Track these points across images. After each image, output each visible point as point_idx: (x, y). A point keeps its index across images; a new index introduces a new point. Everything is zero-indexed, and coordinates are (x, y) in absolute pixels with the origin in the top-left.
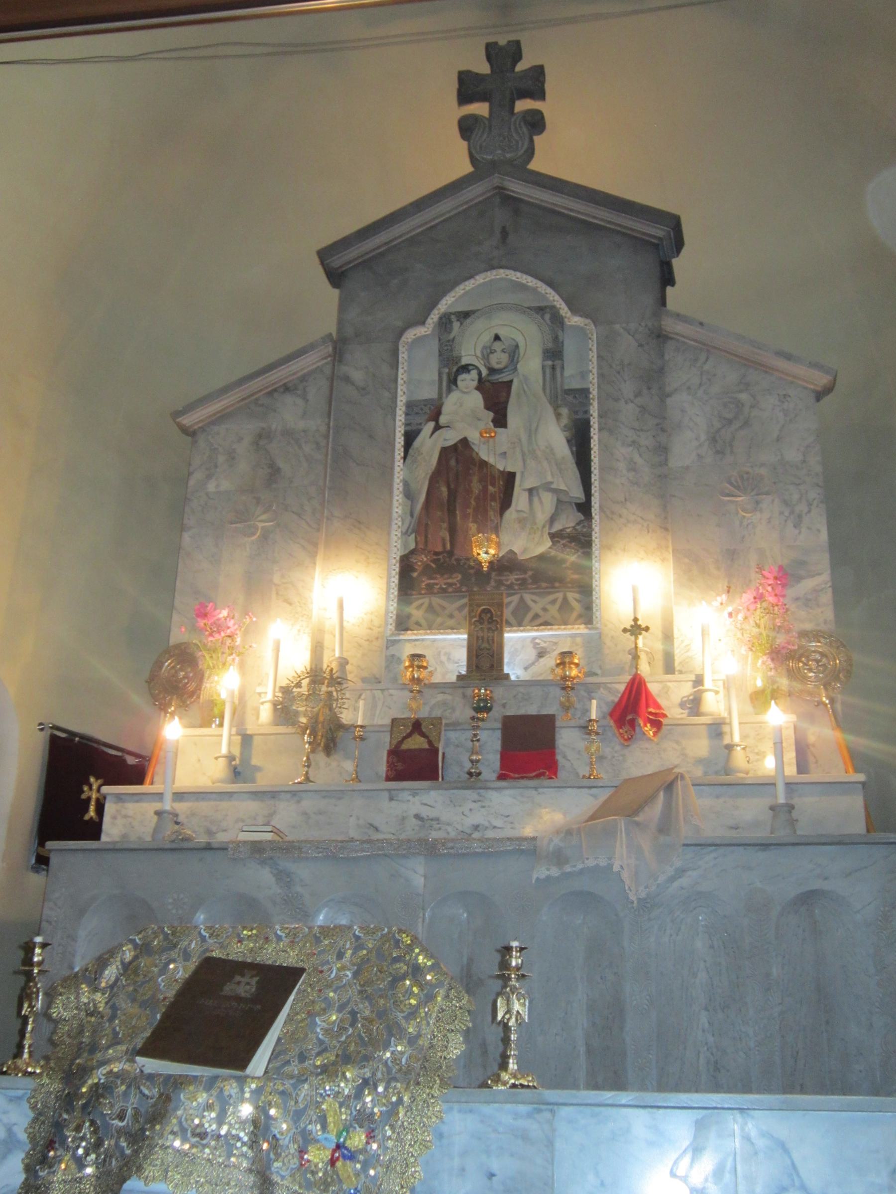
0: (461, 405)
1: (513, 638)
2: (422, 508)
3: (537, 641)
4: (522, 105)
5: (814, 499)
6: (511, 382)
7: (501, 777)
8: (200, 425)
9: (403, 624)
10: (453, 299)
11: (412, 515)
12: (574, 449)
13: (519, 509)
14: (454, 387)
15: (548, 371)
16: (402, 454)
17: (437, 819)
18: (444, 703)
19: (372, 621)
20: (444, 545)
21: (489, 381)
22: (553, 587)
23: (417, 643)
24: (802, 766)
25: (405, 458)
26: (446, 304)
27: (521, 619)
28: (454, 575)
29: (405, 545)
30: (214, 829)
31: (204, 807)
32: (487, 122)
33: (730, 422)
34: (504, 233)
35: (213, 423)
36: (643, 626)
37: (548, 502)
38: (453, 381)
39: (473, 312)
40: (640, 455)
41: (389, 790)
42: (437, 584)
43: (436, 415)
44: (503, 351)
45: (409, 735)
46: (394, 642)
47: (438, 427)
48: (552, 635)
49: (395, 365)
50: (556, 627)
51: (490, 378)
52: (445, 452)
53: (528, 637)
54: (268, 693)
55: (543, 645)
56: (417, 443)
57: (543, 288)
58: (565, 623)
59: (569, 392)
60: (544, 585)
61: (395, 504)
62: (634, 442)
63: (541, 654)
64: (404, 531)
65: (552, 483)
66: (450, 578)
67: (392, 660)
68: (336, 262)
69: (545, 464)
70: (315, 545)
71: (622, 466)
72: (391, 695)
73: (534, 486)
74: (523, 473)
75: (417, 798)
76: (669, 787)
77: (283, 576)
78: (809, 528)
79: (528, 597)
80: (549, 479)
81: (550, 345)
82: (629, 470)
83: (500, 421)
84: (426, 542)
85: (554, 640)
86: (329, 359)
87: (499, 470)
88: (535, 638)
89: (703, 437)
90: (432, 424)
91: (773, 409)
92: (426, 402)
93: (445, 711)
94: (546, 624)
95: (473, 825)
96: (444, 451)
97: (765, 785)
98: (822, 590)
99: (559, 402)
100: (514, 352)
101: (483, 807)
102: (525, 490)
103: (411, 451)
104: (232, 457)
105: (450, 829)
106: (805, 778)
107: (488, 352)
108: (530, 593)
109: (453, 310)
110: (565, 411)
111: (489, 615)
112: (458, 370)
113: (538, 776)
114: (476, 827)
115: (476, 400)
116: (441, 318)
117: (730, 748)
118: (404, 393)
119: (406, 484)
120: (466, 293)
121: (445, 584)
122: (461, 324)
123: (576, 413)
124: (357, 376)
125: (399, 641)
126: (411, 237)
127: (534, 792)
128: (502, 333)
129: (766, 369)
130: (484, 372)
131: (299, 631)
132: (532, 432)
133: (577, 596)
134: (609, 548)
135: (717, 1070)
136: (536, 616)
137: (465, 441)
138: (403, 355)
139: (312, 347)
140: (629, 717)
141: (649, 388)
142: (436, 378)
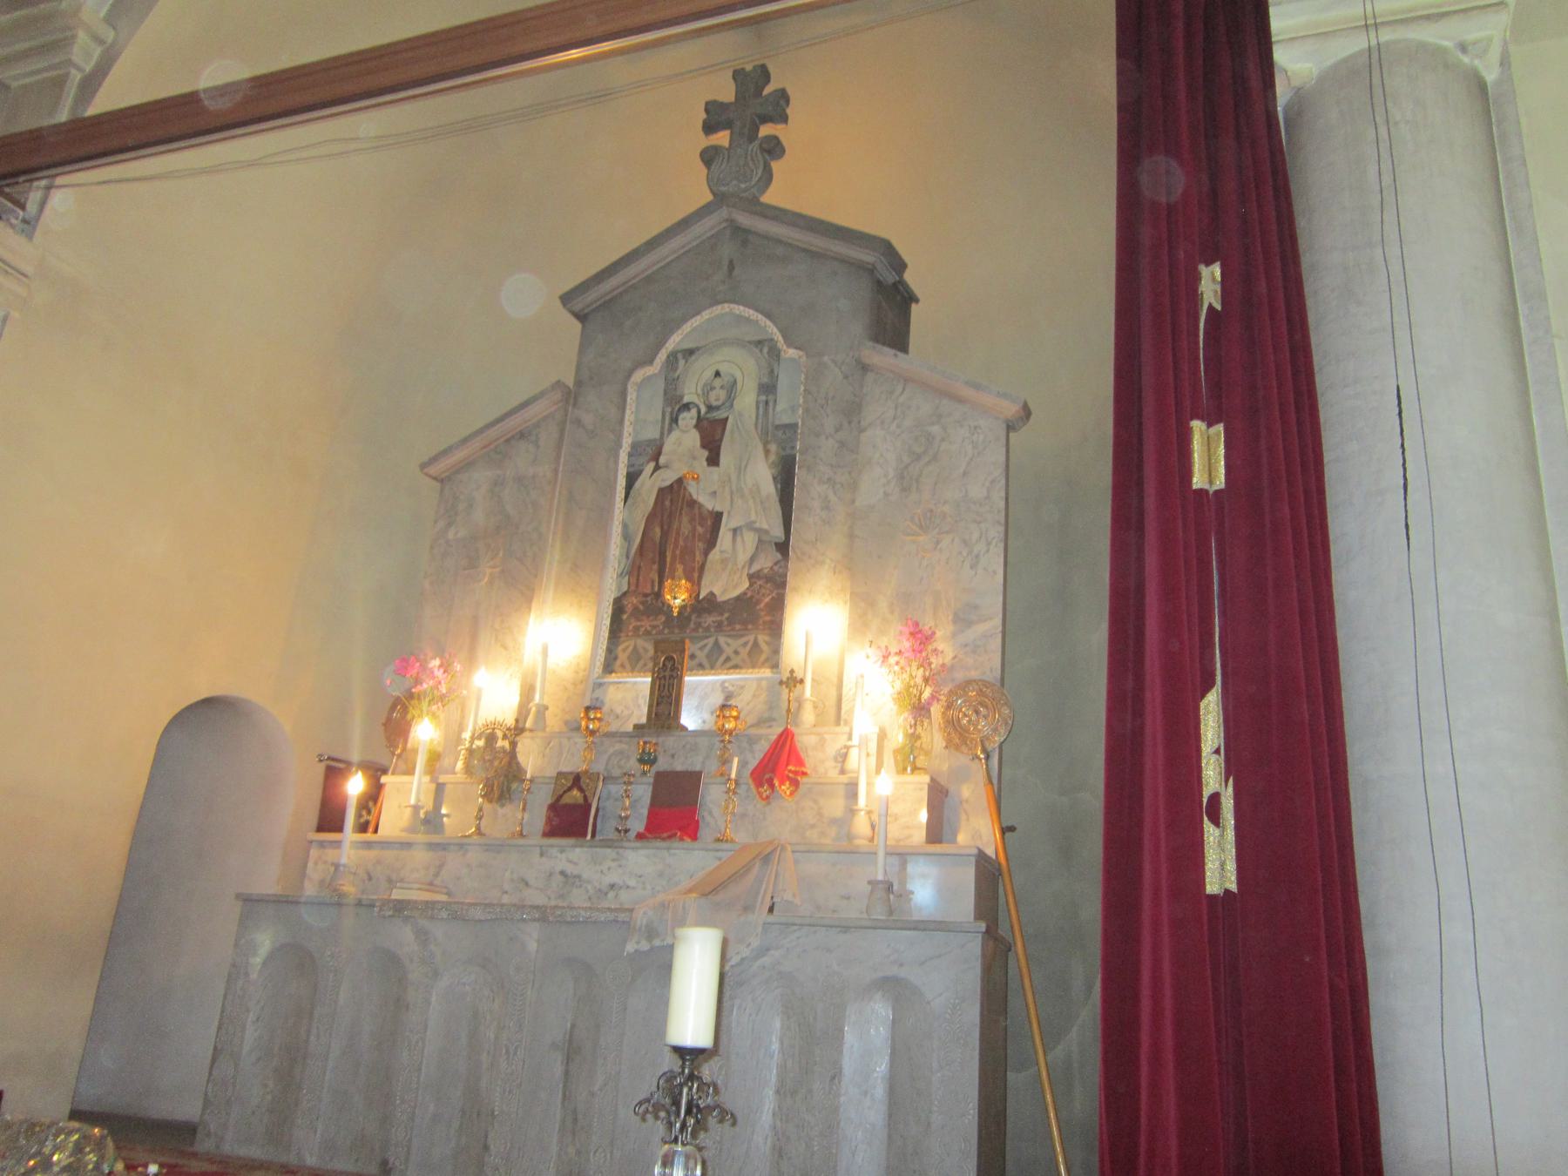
0: (680, 444)
2: (637, 549)
3: (726, 685)
4: (765, 130)
5: (994, 538)
6: (727, 419)
8: (447, 474)
10: (680, 337)
11: (627, 557)
12: (779, 486)
13: (723, 549)
14: (674, 425)
15: (761, 405)
16: (623, 496)
17: (579, 877)
18: (621, 752)
19: (578, 664)
20: (653, 586)
21: (707, 419)
22: (746, 629)
23: (620, 686)
26: (674, 342)
27: (713, 661)
28: (659, 617)
29: (619, 587)
30: (394, 877)
32: (726, 152)
33: (918, 457)
34: (731, 266)
35: (458, 472)
36: (798, 678)
37: (750, 539)
38: (675, 420)
39: (698, 349)
40: (835, 493)
41: (541, 847)
42: (642, 626)
43: (656, 457)
44: (722, 387)
45: (570, 789)
46: (601, 685)
47: (657, 468)
48: (741, 679)
49: (622, 408)
50: (744, 671)
51: (709, 416)
52: (662, 492)
53: (717, 681)
55: (731, 688)
56: (637, 484)
58: (754, 667)
59: (777, 427)
60: (738, 627)
61: (613, 546)
62: (829, 479)
64: (619, 573)
65: (754, 522)
66: (656, 619)
68: (578, 305)
69: (751, 502)
72: (576, 743)
73: (739, 525)
74: (729, 513)
75: (564, 855)
77: (502, 621)
78: (985, 569)
79: (722, 640)
80: (753, 518)
81: (765, 380)
82: (822, 509)
83: (713, 460)
84: (637, 586)
85: (742, 683)
86: (560, 405)
87: (708, 511)
88: (724, 682)
89: (891, 474)
90: (652, 465)
91: (963, 442)
92: (650, 442)
93: (621, 760)
94: (736, 667)
95: (610, 885)
96: (661, 491)
98: (991, 636)
99: (769, 438)
100: (731, 388)
101: (620, 866)
102: (729, 530)
103: (632, 492)
105: (589, 887)
108: (725, 636)
109: (680, 348)
110: (773, 447)
111: (671, 663)
112: (679, 410)
113: (670, 837)
114: (612, 886)
116: (668, 357)
118: (630, 434)
119: (625, 526)
120: (694, 330)
121: (650, 626)
122: (686, 362)
123: (784, 449)
124: (588, 419)
125: (605, 683)
126: (647, 276)
127: (665, 853)
128: (723, 368)
129: (960, 400)
130: (703, 410)
131: (511, 675)
132: (741, 470)
133: (767, 638)
135: (781, 1156)
136: (728, 659)
138: (631, 396)
139: (542, 394)
140: (767, 776)
141: (850, 423)
142: (660, 417)
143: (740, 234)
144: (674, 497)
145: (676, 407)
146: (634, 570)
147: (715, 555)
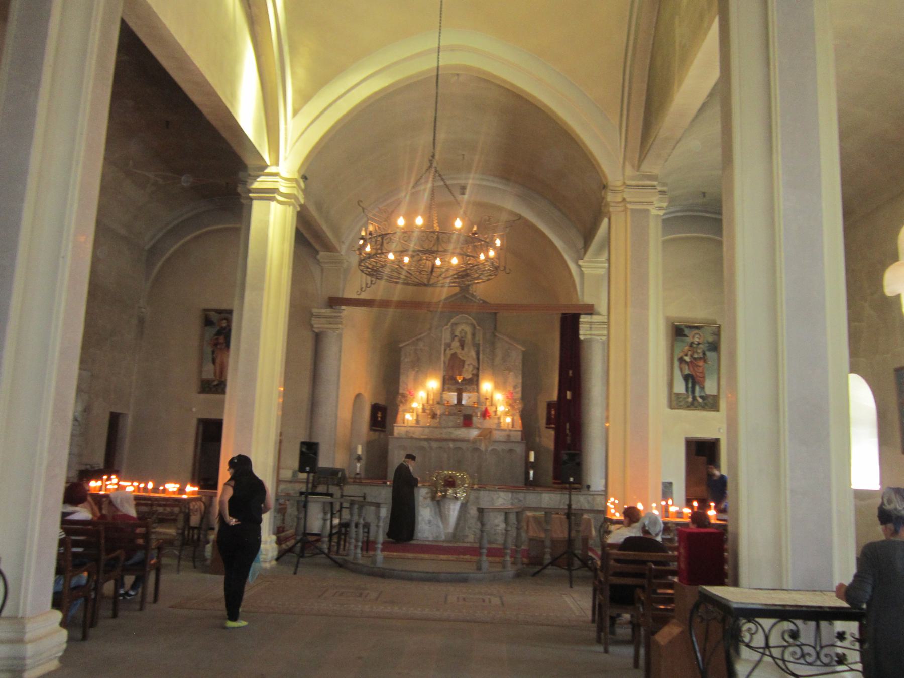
1: (464, 395)
7: (464, 426)
9: (443, 389)
24: (513, 426)
26: (453, 321)
31: (413, 429)
37: (471, 368)
47: (451, 349)
54: (420, 407)
76: (490, 432)
83: (463, 349)
94: (470, 392)
97: (505, 430)
100: (466, 333)
106: (513, 429)
107: (460, 333)
144: (454, 355)
145: (454, 337)
147: (464, 370)
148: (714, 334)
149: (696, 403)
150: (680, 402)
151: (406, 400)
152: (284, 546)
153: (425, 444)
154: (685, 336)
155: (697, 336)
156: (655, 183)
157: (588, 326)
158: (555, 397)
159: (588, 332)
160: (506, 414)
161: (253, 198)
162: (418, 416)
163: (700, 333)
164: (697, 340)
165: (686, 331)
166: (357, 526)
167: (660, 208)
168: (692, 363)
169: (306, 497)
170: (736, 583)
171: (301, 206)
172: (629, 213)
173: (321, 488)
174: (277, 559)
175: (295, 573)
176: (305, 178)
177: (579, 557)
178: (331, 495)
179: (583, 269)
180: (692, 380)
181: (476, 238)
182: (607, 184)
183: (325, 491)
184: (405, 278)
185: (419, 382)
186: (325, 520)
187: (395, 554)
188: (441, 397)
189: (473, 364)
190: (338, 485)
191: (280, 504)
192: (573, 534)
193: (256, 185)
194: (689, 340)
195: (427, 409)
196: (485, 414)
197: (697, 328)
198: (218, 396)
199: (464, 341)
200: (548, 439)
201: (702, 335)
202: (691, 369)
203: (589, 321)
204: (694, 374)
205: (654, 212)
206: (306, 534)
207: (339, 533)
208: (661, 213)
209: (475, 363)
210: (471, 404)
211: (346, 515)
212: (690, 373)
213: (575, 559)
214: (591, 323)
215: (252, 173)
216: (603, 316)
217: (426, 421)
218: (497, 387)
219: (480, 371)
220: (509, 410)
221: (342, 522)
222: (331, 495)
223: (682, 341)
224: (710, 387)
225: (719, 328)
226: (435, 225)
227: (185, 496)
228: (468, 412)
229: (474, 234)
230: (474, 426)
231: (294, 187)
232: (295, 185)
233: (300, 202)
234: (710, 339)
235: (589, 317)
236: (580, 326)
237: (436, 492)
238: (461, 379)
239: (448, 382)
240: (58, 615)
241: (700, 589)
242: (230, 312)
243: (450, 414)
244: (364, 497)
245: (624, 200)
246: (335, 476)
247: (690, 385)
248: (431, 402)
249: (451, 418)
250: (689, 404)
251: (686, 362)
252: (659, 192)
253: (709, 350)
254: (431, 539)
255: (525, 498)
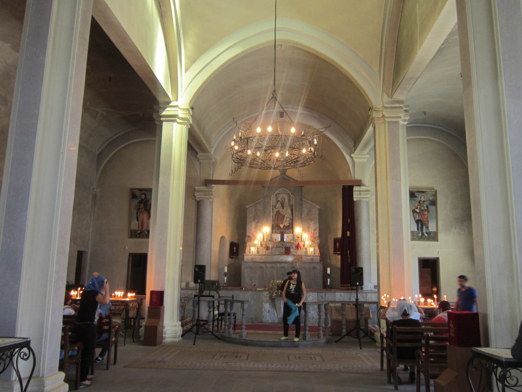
9: (272, 233)
24: (314, 253)
25: (272, 212)
31: (255, 256)
37: (288, 220)
38: (278, 203)
47: (276, 209)
52: (277, 212)
57: (289, 192)
63: (288, 237)
67: (271, 238)
70: (263, 225)
71: (297, 216)
76: (302, 257)
83: (283, 208)
90: (275, 208)
94: (288, 234)
97: (310, 256)
100: (285, 199)
104: (252, 212)
106: (315, 255)
107: (281, 199)
110: (290, 207)
115: (280, 205)
117: (307, 252)
119: (272, 215)
124: (266, 202)
128: (283, 197)
134: (295, 226)
137: (279, 211)
138: (271, 199)
143: (284, 178)
144: (278, 212)
146: (273, 221)
147: (284, 220)
148: (433, 195)
149: (424, 237)
150: (414, 236)
151: (251, 240)
152: (185, 328)
153: (263, 265)
154: (416, 197)
155: (423, 197)
156: (402, 105)
157: (358, 193)
158: (339, 235)
159: (359, 196)
160: (310, 246)
161: (162, 121)
162: (258, 248)
163: (425, 195)
164: (423, 199)
165: (416, 194)
166: (229, 315)
167: (405, 120)
168: (421, 212)
169: (199, 298)
170: (487, 345)
171: (191, 125)
172: (386, 124)
173: (206, 293)
174: (182, 336)
175: (194, 344)
176: (192, 108)
177: (363, 330)
178: (213, 297)
179: (354, 159)
180: (421, 223)
181: (303, 138)
182: (372, 107)
183: (208, 294)
184: (261, 164)
185: (257, 228)
186: (210, 312)
187: (252, 331)
188: (271, 238)
189: (290, 217)
190: (216, 290)
191: (183, 303)
192: (359, 316)
193: (164, 113)
194: (419, 199)
195: (264, 245)
196: (298, 247)
197: (423, 192)
198: (146, 240)
199: (284, 204)
200: (337, 260)
201: (426, 196)
202: (420, 217)
203: (359, 189)
204: (422, 220)
205: (401, 123)
206: (198, 320)
207: (218, 319)
208: (406, 123)
209: (291, 217)
210: (289, 241)
211: (222, 309)
212: (419, 219)
213: (361, 331)
214: (360, 191)
215: (162, 106)
216: (367, 186)
217: (263, 251)
218: (304, 230)
219: (294, 221)
220: (312, 244)
221: (220, 312)
222: (213, 297)
223: (414, 200)
224: (432, 227)
225: (436, 192)
226: (279, 132)
227: (128, 299)
228: (288, 245)
229: (303, 136)
230: (291, 254)
231: (187, 114)
232: (187, 113)
233: (190, 122)
234: (431, 198)
235: (359, 187)
236: (354, 193)
237: (273, 293)
238: (283, 226)
239: (275, 228)
240: (63, 375)
241: (473, 349)
242: (150, 190)
243: (277, 247)
244: (233, 297)
245: (383, 116)
246: (214, 285)
247: (420, 226)
248: (265, 240)
249: (278, 249)
250: (420, 237)
251: (417, 212)
252: (404, 110)
253: (430, 205)
254: (270, 321)
255: (325, 296)
